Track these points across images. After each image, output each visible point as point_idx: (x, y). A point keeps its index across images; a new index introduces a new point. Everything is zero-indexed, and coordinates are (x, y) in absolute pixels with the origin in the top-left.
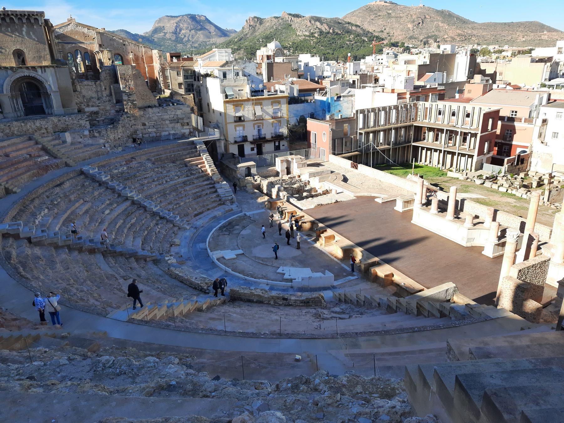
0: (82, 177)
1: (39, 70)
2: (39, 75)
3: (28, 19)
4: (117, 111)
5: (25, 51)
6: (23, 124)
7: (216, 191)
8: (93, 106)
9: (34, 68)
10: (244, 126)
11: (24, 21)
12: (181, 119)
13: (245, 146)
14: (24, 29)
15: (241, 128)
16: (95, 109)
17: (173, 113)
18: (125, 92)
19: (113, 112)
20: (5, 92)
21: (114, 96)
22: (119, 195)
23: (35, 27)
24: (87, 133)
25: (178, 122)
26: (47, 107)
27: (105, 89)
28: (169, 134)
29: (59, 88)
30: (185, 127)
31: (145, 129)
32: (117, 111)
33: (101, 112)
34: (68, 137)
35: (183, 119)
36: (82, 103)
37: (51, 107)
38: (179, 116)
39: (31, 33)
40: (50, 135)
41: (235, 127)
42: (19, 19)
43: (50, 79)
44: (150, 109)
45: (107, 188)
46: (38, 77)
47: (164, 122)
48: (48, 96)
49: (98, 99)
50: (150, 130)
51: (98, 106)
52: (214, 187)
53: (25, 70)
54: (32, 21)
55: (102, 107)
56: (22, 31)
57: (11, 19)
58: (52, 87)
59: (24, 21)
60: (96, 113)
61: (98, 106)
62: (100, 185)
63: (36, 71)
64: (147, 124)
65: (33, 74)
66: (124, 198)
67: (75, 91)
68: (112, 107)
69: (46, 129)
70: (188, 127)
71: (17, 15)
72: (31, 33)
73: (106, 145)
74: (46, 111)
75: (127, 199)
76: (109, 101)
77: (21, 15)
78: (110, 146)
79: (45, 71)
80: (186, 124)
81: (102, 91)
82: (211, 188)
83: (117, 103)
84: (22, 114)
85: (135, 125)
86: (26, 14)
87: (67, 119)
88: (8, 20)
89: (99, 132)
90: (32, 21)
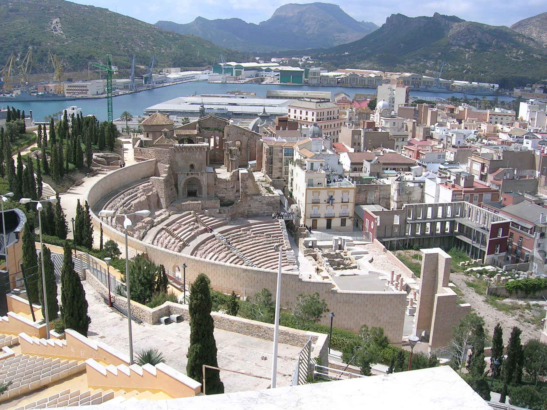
1: (200, 175)
2: (199, 177)
5: (195, 164)
15: (317, 208)
24: (218, 211)
28: (264, 213)
37: (201, 193)
46: (199, 178)
60: (224, 197)
73: (227, 219)
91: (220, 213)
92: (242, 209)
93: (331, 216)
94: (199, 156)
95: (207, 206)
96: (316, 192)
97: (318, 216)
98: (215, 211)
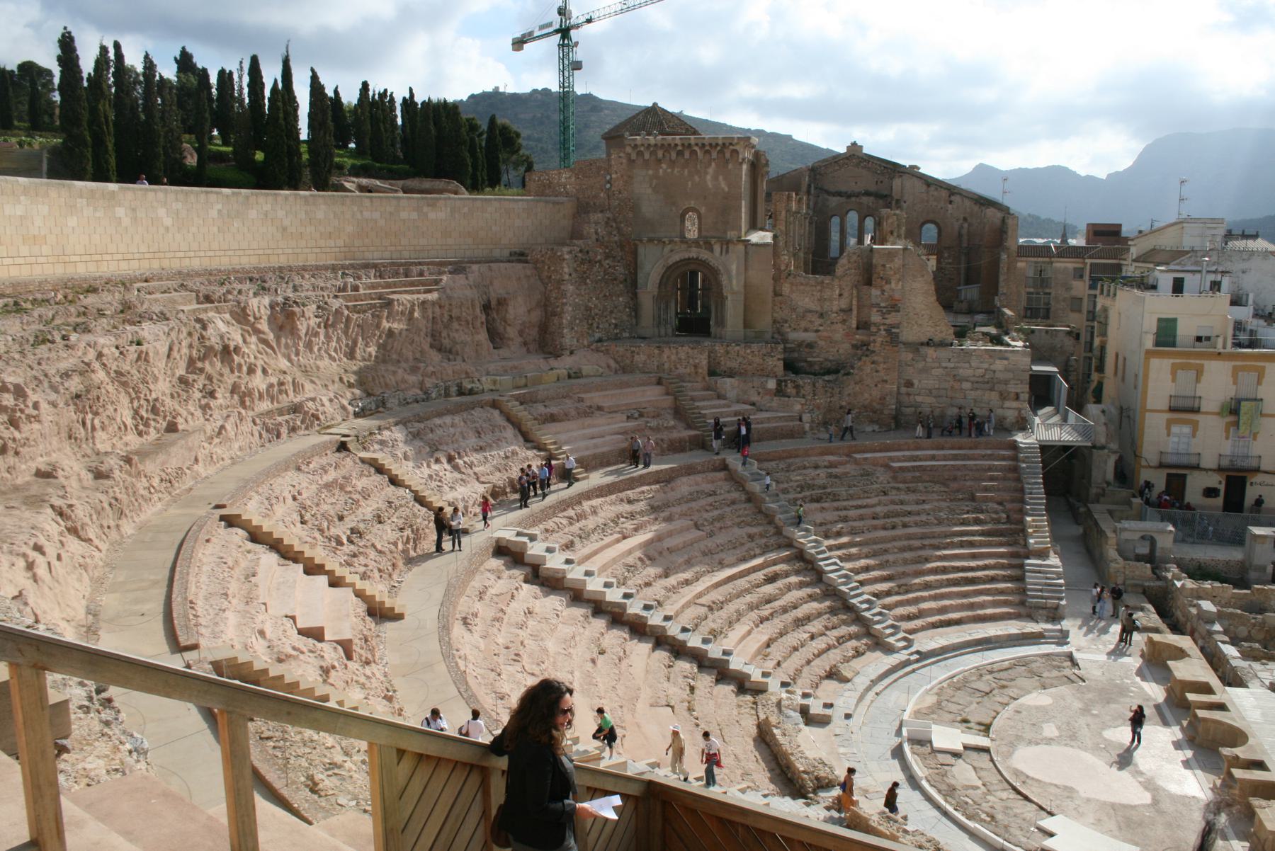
0: (722, 475)
1: (717, 248)
2: (714, 257)
3: (721, 152)
4: (855, 347)
6: (656, 351)
7: (1020, 579)
8: (806, 330)
10: (1195, 426)
11: (714, 155)
12: (999, 382)
13: (1189, 480)
14: (711, 170)
15: (1186, 430)
16: (810, 337)
17: (986, 366)
19: (845, 348)
20: (649, 286)
21: (855, 312)
22: (779, 532)
23: (730, 166)
24: (772, 384)
25: (992, 390)
26: (716, 322)
27: (840, 295)
29: (745, 286)
30: (1007, 404)
31: (909, 394)
32: (855, 347)
33: (821, 343)
34: (729, 385)
35: (1006, 382)
36: (786, 321)
37: (721, 323)
38: (998, 375)
39: (721, 178)
40: (700, 379)
41: (1169, 423)
42: (707, 152)
43: (734, 267)
44: (930, 352)
45: (760, 512)
46: (713, 262)
47: (957, 385)
48: (721, 299)
49: (821, 316)
50: (919, 399)
51: (817, 331)
52: (1022, 566)
54: (728, 155)
55: (825, 334)
56: (706, 173)
57: (694, 153)
58: (734, 282)
59: (714, 155)
60: (810, 346)
61: (817, 331)
62: (749, 500)
64: (916, 382)
66: (781, 540)
67: (777, 294)
68: (847, 335)
69: (696, 366)
70: (1015, 404)
71: (704, 145)
72: (721, 178)
73: (806, 417)
74: (712, 330)
75: (789, 544)
76: (844, 321)
77: (710, 145)
78: (813, 421)
79: (727, 251)
80: (1012, 395)
81: (831, 300)
82: (1011, 566)
83: (858, 328)
84: (670, 331)
85: (886, 381)
86: (720, 142)
87: (742, 353)
88: (687, 155)
89: (797, 387)
90: (728, 155)
91: (780, 392)
92: (876, 393)
93: (1245, 464)
94: (715, 178)
95: (734, 365)
96: (1184, 367)
97: (1194, 461)
98: (763, 386)
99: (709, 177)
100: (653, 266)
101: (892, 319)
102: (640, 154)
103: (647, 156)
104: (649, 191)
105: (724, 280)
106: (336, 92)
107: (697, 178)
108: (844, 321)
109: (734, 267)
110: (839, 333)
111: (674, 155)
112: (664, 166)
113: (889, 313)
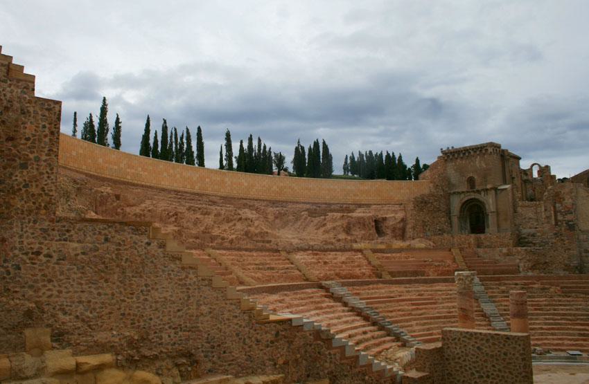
1: (483, 193)
2: (482, 197)
8: (530, 228)
9: (478, 192)
18: (560, 211)
23: (486, 156)
42: (475, 152)
43: (491, 201)
46: (481, 199)
53: (472, 194)
54: (484, 152)
59: (478, 153)
60: (533, 235)
61: (536, 228)
63: (480, 194)
65: (477, 196)
85: (570, 249)
90: (484, 152)
98: (501, 251)
99: (477, 162)
100: (456, 203)
101: (569, 217)
102: (448, 156)
103: (451, 157)
104: (453, 172)
105: (487, 206)
106: (393, 153)
107: (472, 163)
108: (548, 222)
109: (491, 201)
110: (547, 227)
111: (462, 155)
112: (458, 160)
113: (566, 214)
